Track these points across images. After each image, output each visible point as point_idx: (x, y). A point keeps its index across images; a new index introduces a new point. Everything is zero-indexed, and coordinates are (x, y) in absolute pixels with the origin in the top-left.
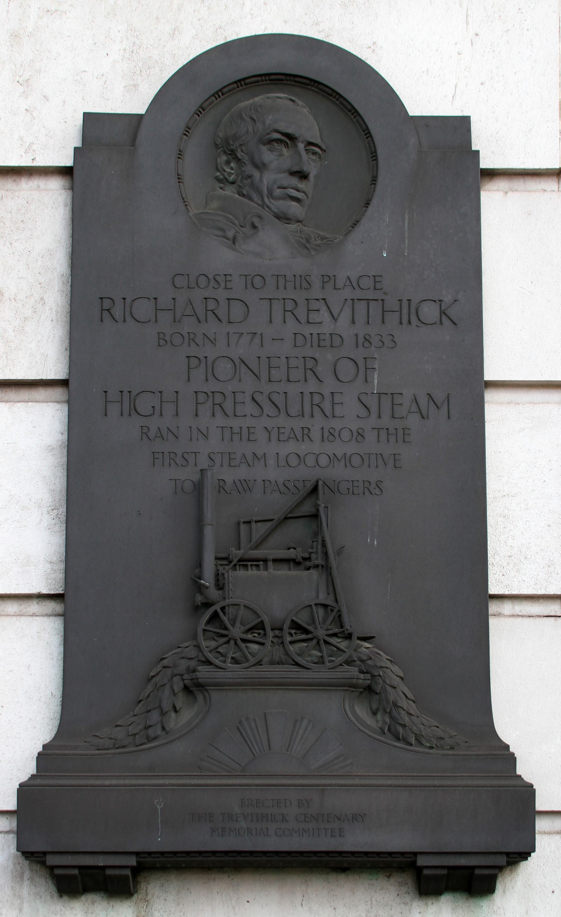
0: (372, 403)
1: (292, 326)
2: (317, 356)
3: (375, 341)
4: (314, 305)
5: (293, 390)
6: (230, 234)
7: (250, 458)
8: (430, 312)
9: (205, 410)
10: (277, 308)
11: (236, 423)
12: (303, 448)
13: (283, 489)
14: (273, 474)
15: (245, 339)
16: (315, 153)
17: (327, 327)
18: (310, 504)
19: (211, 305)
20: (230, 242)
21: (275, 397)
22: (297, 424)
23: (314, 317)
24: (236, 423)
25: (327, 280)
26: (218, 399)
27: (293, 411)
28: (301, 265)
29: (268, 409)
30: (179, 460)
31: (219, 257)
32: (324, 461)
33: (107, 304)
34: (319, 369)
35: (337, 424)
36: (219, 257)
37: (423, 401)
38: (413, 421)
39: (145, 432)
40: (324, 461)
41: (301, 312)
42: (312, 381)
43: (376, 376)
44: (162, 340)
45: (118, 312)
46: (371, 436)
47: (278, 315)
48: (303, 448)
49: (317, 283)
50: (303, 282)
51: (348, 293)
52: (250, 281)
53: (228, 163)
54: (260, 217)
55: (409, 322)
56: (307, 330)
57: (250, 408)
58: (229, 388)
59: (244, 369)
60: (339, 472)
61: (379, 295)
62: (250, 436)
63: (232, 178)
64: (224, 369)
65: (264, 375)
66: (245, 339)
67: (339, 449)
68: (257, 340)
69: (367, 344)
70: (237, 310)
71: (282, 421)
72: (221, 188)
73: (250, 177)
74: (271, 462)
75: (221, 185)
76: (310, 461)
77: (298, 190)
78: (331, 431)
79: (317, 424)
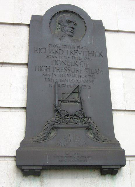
0: (88, 70)
1: (72, 55)
2: (77, 61)
3: (88, 59)
4: (76, 52)
5: (73, 67)
6: (60, 38)
7: (64, 80)
8: (97, 54)
9: (55, 71)
11: (62, 73)
12: (75, 79)
14: (69, 83)
15: (63, 57)
17: (79, 56)
18: (77, 89)
19: (56, 50)
21: (69, 69)
22: (74, 74)
24: (62, 73)
25: (78, 47)
26: (58, 68)
27: (73, 71)
28: (73, 44)
29: (68, 71)
30: (50, 80)
31: (58, 42)
32: (79, 81)
33: (36, 49)
34: (77, 64)
35: (81, 74)
36: (58, 42)
37: (97, 70)
38: (96, 74)
39: (43, 74)
40: (79, 81)
41: (74, 53)
42: (76, 66)
44: (47, 57)
45: (38, 50)
47: (69, 53)
48: (75, 79)
49: (76, 48)
50: (74, 47)
51: (82, 50)
52: (64, 46)
56: (75, 56)
57: (64, 70)
58: (60, 66)
59: (63, 63)
60: (81, 84)
62: (64, 76)
64: (59, 63)
65: (67, 64)
66: (63, 57)
67: (82, 79)
68: (65, 57)
70: (61, 52)
71: (71, 73)
74: (69, 81)
76: (76, 81)
79: (77, 74)
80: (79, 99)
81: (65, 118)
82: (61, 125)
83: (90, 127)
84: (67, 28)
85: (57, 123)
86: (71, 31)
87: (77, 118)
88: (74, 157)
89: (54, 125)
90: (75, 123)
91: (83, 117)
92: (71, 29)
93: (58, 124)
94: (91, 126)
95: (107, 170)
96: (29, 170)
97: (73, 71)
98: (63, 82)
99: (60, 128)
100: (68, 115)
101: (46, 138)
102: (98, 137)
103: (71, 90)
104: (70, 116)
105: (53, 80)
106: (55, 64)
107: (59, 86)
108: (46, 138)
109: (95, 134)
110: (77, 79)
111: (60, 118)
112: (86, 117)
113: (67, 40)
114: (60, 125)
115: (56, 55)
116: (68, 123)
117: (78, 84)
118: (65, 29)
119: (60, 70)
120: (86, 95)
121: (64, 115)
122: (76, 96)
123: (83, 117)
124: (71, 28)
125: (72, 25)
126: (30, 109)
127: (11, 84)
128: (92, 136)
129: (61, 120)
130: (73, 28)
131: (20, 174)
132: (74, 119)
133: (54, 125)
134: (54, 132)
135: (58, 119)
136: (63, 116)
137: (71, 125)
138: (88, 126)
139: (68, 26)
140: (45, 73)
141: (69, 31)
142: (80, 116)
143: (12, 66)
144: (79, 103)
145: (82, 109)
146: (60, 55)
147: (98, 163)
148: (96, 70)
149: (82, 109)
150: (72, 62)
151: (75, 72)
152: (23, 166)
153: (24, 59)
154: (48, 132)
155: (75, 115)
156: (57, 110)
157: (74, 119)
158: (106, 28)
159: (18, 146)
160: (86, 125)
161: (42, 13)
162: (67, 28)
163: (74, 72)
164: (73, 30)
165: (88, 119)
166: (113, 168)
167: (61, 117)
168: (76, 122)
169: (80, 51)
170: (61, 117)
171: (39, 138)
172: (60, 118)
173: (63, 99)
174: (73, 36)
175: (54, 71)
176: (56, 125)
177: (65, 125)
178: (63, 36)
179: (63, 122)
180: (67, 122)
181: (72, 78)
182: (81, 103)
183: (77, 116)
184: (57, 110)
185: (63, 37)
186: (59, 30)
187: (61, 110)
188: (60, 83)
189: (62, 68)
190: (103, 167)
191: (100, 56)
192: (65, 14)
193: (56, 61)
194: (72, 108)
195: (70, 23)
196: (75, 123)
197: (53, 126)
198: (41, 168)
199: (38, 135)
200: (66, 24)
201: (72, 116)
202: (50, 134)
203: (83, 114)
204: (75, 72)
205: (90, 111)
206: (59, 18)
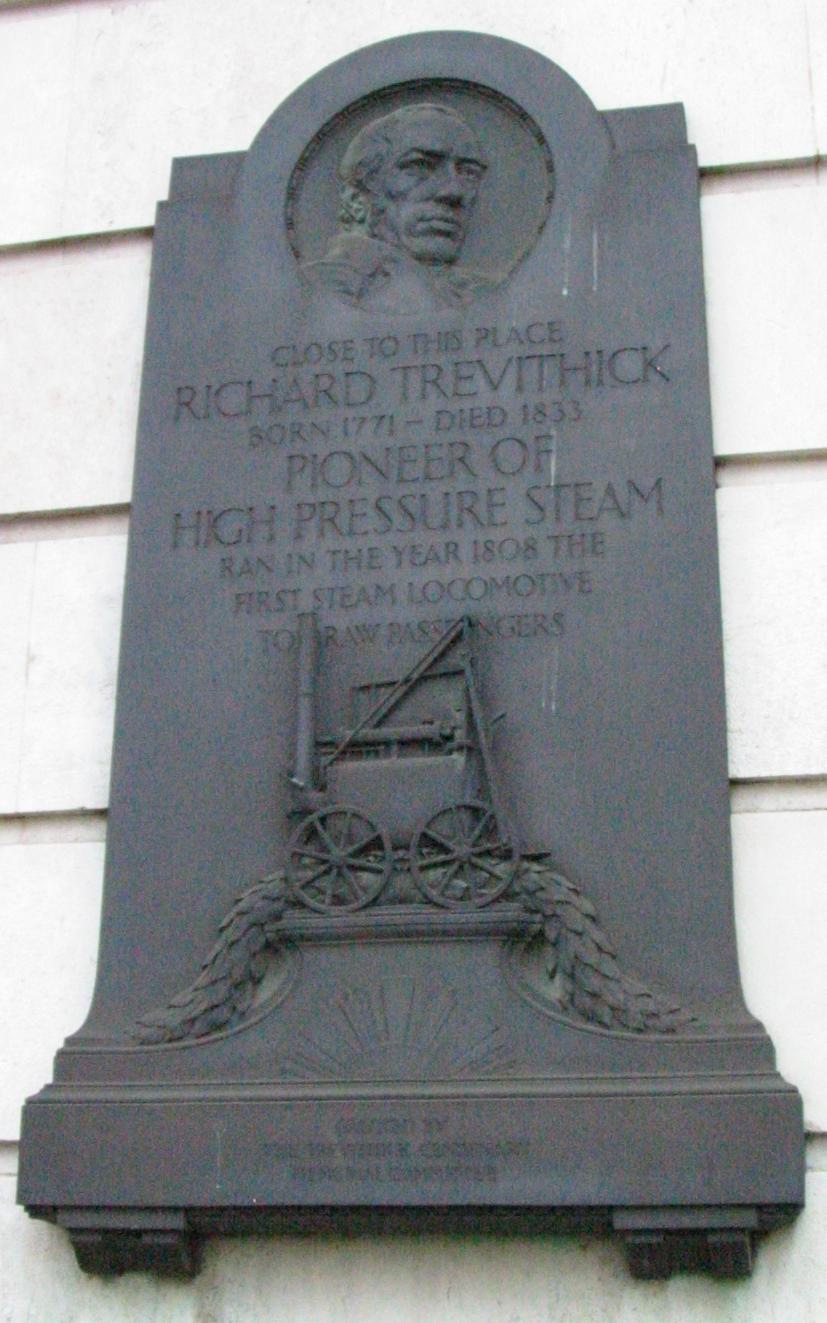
0: (547, 498)
1: (434, 402)
3: (551, 411)
4: (465, 371)
10: (415, 379)
13: (418, 634)
14: (407, 614)
15: (369, 428)
16: (470, 172)
18: (457, 651)
19: (325, 383)
20: (354, 300)
22: (440, 539)
23: (466, 387)
25: (485, 334)
31: (337, 319)
32: (477, 590)
33: (186, 396)
35: (497, 535)
36: (337, 319)
38: (608, 523)
39: (227, 565)
42: (462, 475)
43: (553, 463)
44: (258, 436)
45: (199, 403)
46: (545, 548)
48: (447, 574)
49: (469, 340)
50: (450, 340)
51: (514, 350)
52: (378, 345)
53: (354, 197)
54: (394, 261)
55: (600, 383)
57: (373, 521)
59: (367, 468)
60: (501, 605)
61: (556, 349)
63: (359, 216)
64: (339, 469)
66: (369, 428)
67: (499, 570)
69: (539, 418)
71: (422, 538)
72: (347, 230)
73: (382, 211)
75: (347, 226)
76: (458, 590)
77: (446, 221)
78: (489, 545)
79: (467, 537)
80: (460, 717)
81: (353, 868)
82: (451, 917)
83: (536, 928)
84: (406, 212)
85: (299, 904)
86: (442, 226)
87: (444, 864)
88: (403, 1150)
89: (279, 925)
90: (429, 901)
91: (488, 853)
92: (439, 210)
93: (305, 913)
94: (545, 916)
95: (654, 1240)
96: (660, 1239)
97: (435, 521)
98: (363, 608)
99: (317, 940)
100: (376, 843)
101: (224, 1013)
102: (594, 995)
103: (408, 659)
104: (395, 848)
105: (289, 599)
106: (314, 479)
107: (323, 641)
108: (224, 1013)
109: (578, 972)
110: (466, 571)
111: (323, 868)
112: (507, 855)
113: (409, 301)
114: (314, 922)
115: (324, 414)
116: (374, 902)
117: (454, 609)
118: (398, 216)
119: (343, 520)
120: (533, 685)
121: (350, 849)
122: (445, 702)
123: (488, 853)
124: (442, 200)
125: (448, 182)
126: (141, 822)
127: (31, 659)
128: (555, 990)
129: (325, 883)
130: (454, 203)
131: (68, 1260)
132: (423, 868)
133: (279, 925)
134: (283, 976)
135: (309, 874)
136: (338, 853)
137: (398, 919)
138: (526, 916)
139: (415, 193)
140: (239, 554)
141: (421, 226)
142: (462, 849)
143: (51, 530)
144: (460, 748)
145: (482, 791)
146: (350, 413)
147: (584, 1188)
148: (610, 491)
149: (482, 791)
150: (435, 452)
151: (454, 523)
152: (624, 1208)
153: (111, 477)
154: (237, 974)
155: (427, 841)
156: (305, 812)
157: (423, 868)
158: (705, 160)
159: (39, 1075)
160: (512, 911)
161: (239, 139)
162: (406, 212)
163: (445, 526)
164: (451, 214)
165: (526, 865)
166: (702, 1233)
167: (324, 862)
168: (434, 893)
169: (494, 361)
170: (324, 862)
171: (174, 1019)
172: (323, 868)
173: (349, 734)
174: (451, 261)
175: (366, 533)
176: (294, 920)
177: (352, 919)
178: (378, 272)
179: (338, 900)
180: (364, 899)
181: (431, 573)
182: (471, 750)
183: (443, 848)
184: (305, 812)
185: (380, 277)
186: (359, 232)
187: (329, 809)
188: (340, 621)
189: (358, 508)
190: (621, 1221)
191: (646, 380)
192: (398, 113)
193: (320, 459)
194: (401, 791)
195: (431, 167)
196: (429, 901)
197: (266, 928)
198: (178, 1222)
199: (174, 1001)
200: (404, 181)
201: (407, 847)
202: (249, 986)
203: (490, 831)
204: (454, 523)
205: (551, 803)
206: (353, 150)
